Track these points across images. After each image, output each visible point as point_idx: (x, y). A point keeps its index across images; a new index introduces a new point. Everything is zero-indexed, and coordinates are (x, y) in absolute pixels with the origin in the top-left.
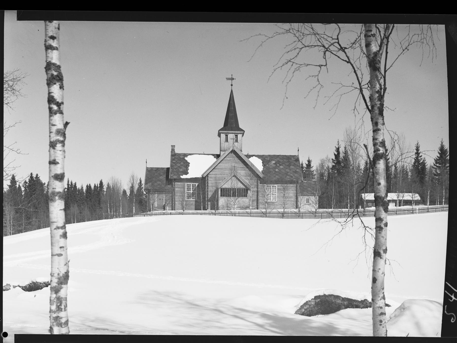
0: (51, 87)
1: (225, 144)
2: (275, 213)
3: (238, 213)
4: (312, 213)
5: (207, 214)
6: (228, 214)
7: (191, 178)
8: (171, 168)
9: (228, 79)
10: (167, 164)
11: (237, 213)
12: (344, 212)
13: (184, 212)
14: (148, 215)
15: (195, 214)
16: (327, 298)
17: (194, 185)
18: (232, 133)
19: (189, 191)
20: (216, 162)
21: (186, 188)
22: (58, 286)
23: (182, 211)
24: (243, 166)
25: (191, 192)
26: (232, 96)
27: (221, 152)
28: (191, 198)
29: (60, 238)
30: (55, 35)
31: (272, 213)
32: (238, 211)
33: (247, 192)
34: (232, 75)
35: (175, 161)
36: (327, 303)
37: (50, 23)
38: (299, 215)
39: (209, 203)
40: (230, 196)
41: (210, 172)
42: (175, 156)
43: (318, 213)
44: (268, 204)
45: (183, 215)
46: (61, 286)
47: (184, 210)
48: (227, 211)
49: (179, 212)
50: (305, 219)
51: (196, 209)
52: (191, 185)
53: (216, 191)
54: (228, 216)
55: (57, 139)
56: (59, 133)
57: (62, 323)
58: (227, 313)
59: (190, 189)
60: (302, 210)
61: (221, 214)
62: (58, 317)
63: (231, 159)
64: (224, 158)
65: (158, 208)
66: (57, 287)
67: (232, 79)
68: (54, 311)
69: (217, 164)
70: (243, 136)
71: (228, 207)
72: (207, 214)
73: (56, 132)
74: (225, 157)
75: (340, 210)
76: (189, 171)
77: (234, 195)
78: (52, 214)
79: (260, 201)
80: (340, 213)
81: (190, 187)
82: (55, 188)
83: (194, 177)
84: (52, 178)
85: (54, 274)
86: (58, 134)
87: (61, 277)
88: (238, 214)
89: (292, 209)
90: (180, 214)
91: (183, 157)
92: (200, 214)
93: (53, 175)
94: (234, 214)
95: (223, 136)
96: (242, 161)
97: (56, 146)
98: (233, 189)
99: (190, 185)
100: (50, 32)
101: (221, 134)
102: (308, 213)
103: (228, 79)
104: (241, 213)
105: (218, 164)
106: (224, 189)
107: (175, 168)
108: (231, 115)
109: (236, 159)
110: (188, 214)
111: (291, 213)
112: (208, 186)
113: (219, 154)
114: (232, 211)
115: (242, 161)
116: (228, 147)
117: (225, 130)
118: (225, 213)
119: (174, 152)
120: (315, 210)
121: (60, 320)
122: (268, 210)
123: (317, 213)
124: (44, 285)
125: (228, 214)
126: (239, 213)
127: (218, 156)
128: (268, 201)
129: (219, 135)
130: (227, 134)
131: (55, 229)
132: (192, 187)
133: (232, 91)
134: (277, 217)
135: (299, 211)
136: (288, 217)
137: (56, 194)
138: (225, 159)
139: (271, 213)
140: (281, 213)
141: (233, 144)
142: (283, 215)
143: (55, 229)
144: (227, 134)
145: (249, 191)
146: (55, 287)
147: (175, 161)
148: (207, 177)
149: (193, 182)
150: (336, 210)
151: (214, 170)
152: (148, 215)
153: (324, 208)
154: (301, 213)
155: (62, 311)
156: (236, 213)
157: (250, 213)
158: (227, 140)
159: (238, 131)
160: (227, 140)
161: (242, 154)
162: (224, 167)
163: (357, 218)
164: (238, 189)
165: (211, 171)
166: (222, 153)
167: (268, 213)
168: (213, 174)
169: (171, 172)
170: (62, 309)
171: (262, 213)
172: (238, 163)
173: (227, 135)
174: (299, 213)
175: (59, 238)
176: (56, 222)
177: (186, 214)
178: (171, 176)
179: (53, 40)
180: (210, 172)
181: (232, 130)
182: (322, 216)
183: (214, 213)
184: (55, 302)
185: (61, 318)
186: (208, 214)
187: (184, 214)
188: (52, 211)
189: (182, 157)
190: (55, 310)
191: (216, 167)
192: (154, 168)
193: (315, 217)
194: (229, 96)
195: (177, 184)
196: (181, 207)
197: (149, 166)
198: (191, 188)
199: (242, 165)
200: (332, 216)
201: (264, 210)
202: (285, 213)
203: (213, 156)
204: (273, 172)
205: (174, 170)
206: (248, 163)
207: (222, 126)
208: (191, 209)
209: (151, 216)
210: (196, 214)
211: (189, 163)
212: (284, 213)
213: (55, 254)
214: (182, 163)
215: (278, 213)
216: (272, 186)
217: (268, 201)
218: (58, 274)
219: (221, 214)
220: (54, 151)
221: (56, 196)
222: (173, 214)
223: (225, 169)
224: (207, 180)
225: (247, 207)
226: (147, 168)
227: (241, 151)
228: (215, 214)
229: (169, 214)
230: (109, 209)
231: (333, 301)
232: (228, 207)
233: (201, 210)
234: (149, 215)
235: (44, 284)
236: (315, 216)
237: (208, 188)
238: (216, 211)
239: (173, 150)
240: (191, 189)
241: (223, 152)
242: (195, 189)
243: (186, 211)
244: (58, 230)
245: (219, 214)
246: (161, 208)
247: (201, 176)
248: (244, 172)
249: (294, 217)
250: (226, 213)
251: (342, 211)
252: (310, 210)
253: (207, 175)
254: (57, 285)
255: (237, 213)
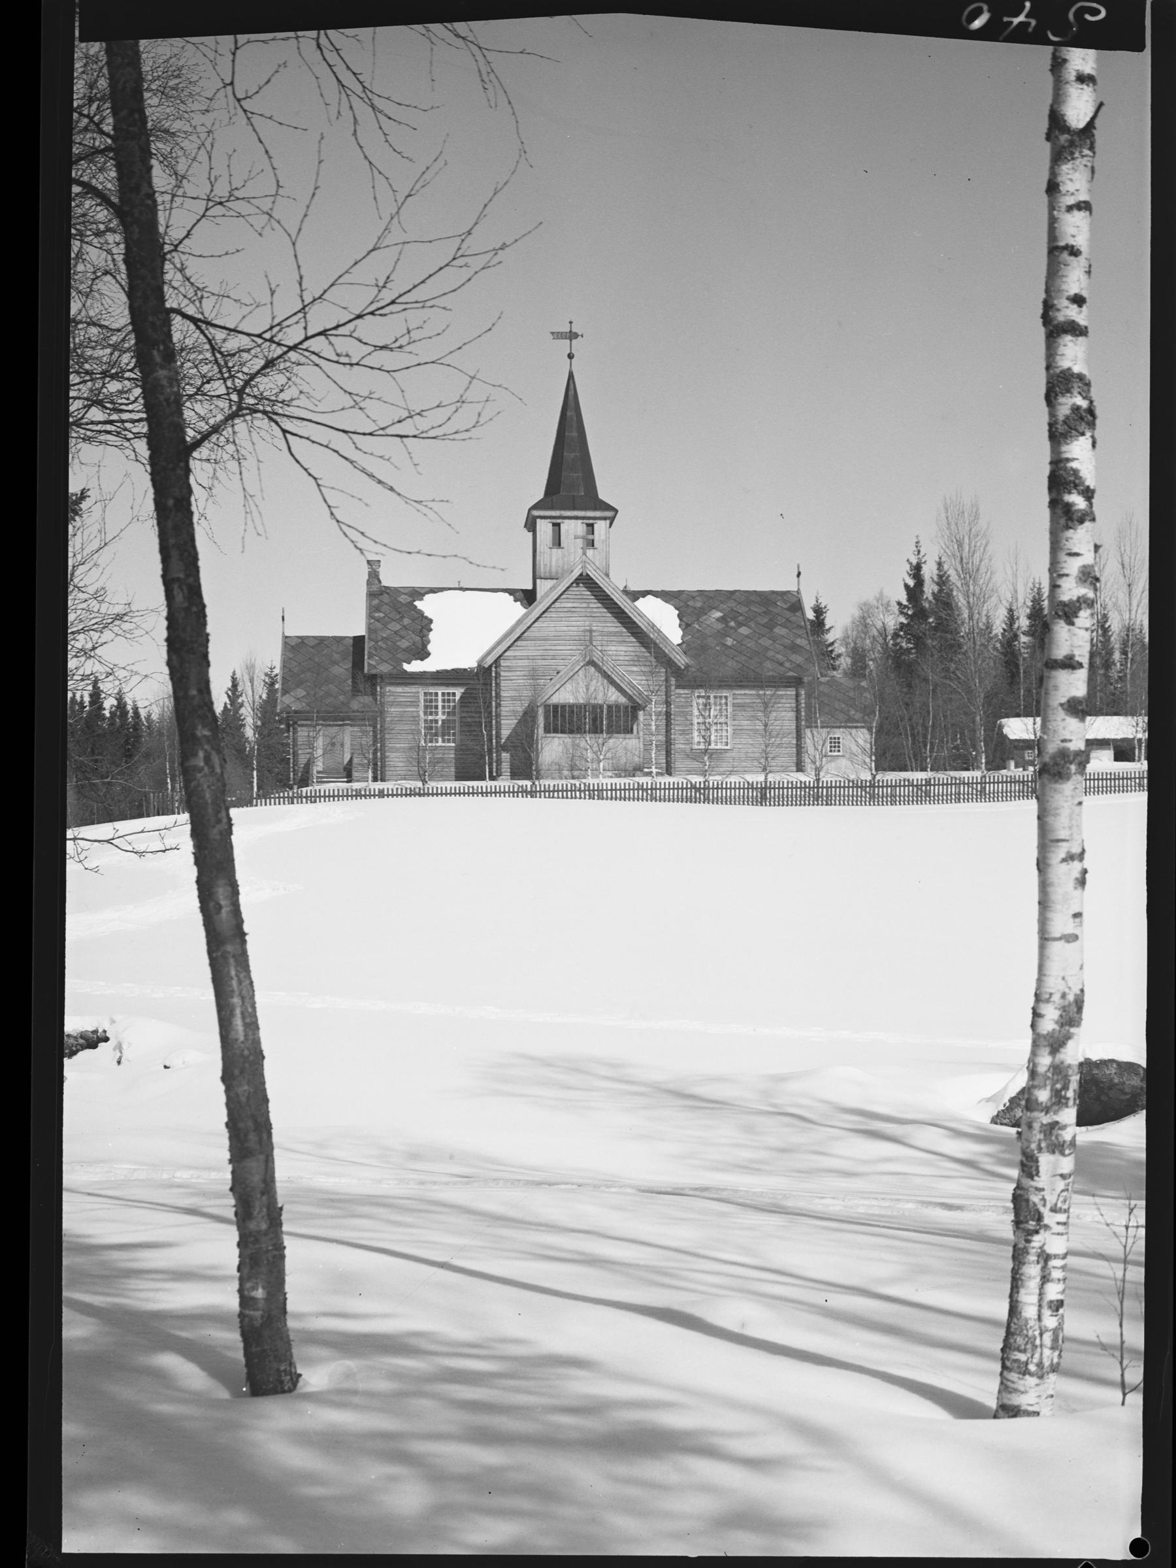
0: (1072, 442)
1: (551, 555)
2: (735, 789)
3: (611, 790)
4: (861, 787)
5: (504, 792)
6: (578, 793)
7: (438, 672)
8: (369, 638)
9: (558, 335)
10: (354, 624)
11: (607, 790)
12: (968, 784)
13: (426, 786)
14: (304, 800)
15: (464, 794)
16: (1095, 1071)
17: (449, 694)
18: (577, 518)
19: (431, 714)
20: (525, 616)
21: (422, 703)
22: (1060, 1031)
23: (420, 784)
24: (617, 630)
25: (441, 717)
26: (571, 393)
27: (538, 581)
28: (440, 739)
29: (1076, 888)
30: (1085, 294)
31: (726, 789)
32: (609, 781)
33: (635, 717)
34: (571, 323)
35: (382, 615)
36: (1094, 1088)
37: (1072, 258)
38: (817, 795)
39: (505, 756)
40: (585, 732)
41: (505, 651)
42: (381, 597)
43: (883, 787)
44: (707, 756)
45: (422, 798)
46: (1068, 1031)
47: (424, 782)
48: (573, 781)
49: (408, 786)
50: (837, 807)
51: (459, 778)
52: (440, 694)
53: (528, 717)
54: (576, 798)
55: (1080, 595)
56: (1089, 577)
57: (1064, 1142)
58: (824, 1123)
59: (436, 707)
60: (826, 778)
61: (554, 791)
62: (1057, 1123)
63: (575, 605)
64: (553, 603)
65: (329, 774)
66: (1056, 1035)
67: (572, 336)
68: (1046, 1107)
69: (528, 625)
70: (611, 524)
71: (575, 768)
72: (504, 792)
73: (1080, 575)
74: (557, 599)
75: (953, 773)
76: (430, 647)
77: (596, 729)
78: (1056, 815)
79: (677, 746)
80: (955, 784)
81: (437, 700)
82: (1070, 741)
83: (449, 668)
84: (1060, 708)
85: (1051, 994)
86: (1085, 581)
87: (1070, 1004)
88: (609, 792)
89: (792, 774)
90: (412, 793)
91: (409, 599)
92: (482, 793)
93: (1064, 700)
94: (596, 793)
95: (544, 528)
96: (616, 610)
97: (1077, 617)
98: (594, 707)
99: (436, 694)
100: (1072, 285)
101: (538, 520)
102: (849, 787)
103: (558, 335)
104: (620, 790)
105: (534, 622)
106: (556, 707)
107: (383, 638)
108: (569, 455)
109: (595, 605)
110: (442, 794)
111: (792, 788)
112: (498, 696)
113: (530, 587)
114: (591, 781)
115: (616, 610)
116: (561, 562)
117: (552, 508)
118: (567, 791)
119: (377, 582)
120: (869, 778)
121: (1060, 1132)
122: (711, 778)
123: (879, 787)
124: (81, 1041)
125: (578, 793)
126: (616, 790)
127: (528, 597)
128: (713, 746)
129: (531, 525)
130: (559, 521)
131: (1064, 860)
132: (444, 701)
133: (571, 376)
134: (744, 801)
135: (818, 780)
136: (781, 801)
137: (1071, 758)
138: (557, 605)
139: (722, 788)
140: (757, 788)
141: (584, 554)
142: (763, 795)
143: (1064, 860)
144: (559, 521)
145: (641, 713)
146: (1051, 1035)
147: (382, 615)
148: (496, 667)
149: (447, 685)
150: (941, 776)
151: (519, 643)
152: (304, 800)
153: (904, 769)
154: (822, 787)
155: (1067, 1107)
156: (602, 790)
157: (652, 789)
158: (557, 542)
159: (595, 509)
160: (557, 542)
161: (615, 588)
162: (553, 634)
163: (1030, 801)
164: (609, 707)
165: (509, 647)
166: (543, 587)
167: (713, 789)
168: (515, 658)
169: (369, 652)
170: (1068, 1099)
171: (693, 787)
172: (602, 619)
173: (559, 525)
174: (818, 787)
175: (1072, 889)
176: (1067, 841)
177: (433, 795)
178: (369, 663)
179: (1080, 306)
180: (505, 651)
181: (574, 509)
182: (893, 796)
183: (529, 789)
184: (1049, 1078)
185: (1064, 1127)
186: (509, 792)
187: (428, 795)
188: (1057, 809)
189: (403, 599)
190: (1049, 1104)
191: (526, 634)
192: (308, 637)
193: (873, 799)
194: (564, 391)
195: (389, 691)
196: (416, 769)
197: (296, 630)
198: (440, 704)
199: (612, 625)
200: (927, 794)
201: (697, 779)
202: (770, 788)
203: (511, 594)
204: (718, 648)
205: (379, 643)
206: (635, 619)
207: (540, 494)
208: (445, 778)
209: (315, 802)
210: (469, 794)
211: (431, 621)
212: (766, 788)
213: (1058, 935)
214: (406, 621)
215: (748, 788)
216: (715, 697)
217: (713, 746)
218: (1064, 996)
219: (554, 791)
220: (1069, 630)
221: (1071, 763)
222: (388, 796)
223: (557, 638)
224: (496, 678)
225: (637, 770)
226: (286, 638)
227: (607, 575)
228: (531, 792)
229: (374, 796)
230: (169, 781)
231: (1116, 1081)
232: (575, 768)
233: (484, 779)
234: (306, 797)
235: (82, 1037)
236: (927, 794)
237: (498, 705)
238: (537, 783)
239: (374, 576)
240: (440, 707)
241: (549, 584)
242: (454, 707)
243: (432, 785)
244: (1070, 862)
245: (545, 792)
246: (338, 773)
247: (476, 665)
248: (624, 648)
249: (855, 801)
250: (571, 791)
251: (960, 779)
252: (852, 777)
253: (497, 662)
254: (1057, 1027)
255: (607, 790)
